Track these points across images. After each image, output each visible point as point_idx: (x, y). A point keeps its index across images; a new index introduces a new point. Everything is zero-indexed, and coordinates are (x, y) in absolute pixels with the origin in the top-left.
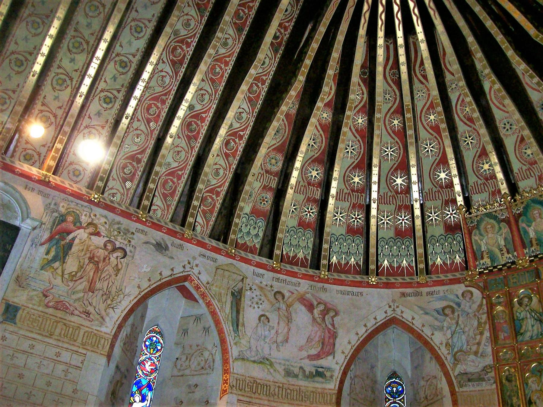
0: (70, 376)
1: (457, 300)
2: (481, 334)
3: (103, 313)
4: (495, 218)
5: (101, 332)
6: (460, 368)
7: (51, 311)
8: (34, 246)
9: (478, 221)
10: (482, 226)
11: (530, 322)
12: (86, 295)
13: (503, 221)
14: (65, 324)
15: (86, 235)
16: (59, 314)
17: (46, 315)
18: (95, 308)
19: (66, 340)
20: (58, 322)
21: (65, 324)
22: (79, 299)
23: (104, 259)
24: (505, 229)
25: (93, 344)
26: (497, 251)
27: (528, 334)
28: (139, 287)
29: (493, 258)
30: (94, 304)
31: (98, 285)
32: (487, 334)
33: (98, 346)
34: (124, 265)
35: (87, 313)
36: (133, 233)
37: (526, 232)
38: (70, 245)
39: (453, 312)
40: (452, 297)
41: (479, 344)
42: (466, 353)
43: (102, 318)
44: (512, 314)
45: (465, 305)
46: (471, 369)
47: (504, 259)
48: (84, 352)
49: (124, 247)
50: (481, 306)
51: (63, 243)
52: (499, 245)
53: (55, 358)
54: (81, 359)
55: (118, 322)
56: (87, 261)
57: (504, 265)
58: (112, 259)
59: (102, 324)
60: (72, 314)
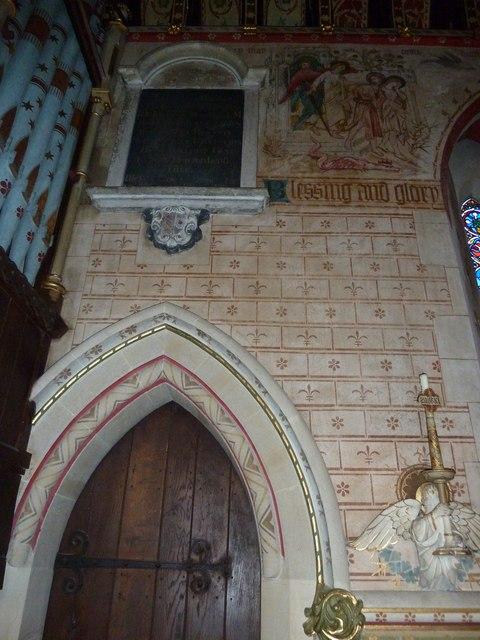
0: (402, 250)
3: (409, 156)
5: (420, 180)
7: (331, 174)
8: (271, 107)
12: (373, 142)
14: (361, 184)
15: (337, 76)
16: (347, 174)
17: (328, 181)
18: (394, 153)
19: (371, 203)
20: (349, 185)
21: (361, 184)
22: (365, 150)
23: (377, 95)
25: (416, 198)
28: (444, 113)
30: (391, 149)
31: (384, 126)
33: (424, 200)
34: (409, 93)
35: (387, 162)
36: (399, 57)
38: (321, 91)
43: (411, 162)
48: (409, 212)
49: (396, 74)
51: (308, 93)
53: (368, 230)
54: (407, 222)
55: (439, 162)
56: (353, 104)
58: (388, 92)
59: (416, 172)
60: (365, 169)
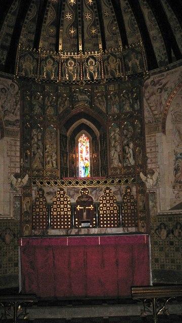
1: (8, 87)
2: (16, 105)
4: (33, 56)
6: (6, 118)
9: (25, 54)
10: (26, 57)
11: (37, 107)
13: (36, 59)
24: (35, 63)
26: (29, 71)
27: (36, 111)
29: (26, 74)
32: (19, 106)
37: (43, 69)
39: (6, 91)
40: (6, 84)
41: (15, 109)
42: (10, 112)
44: (31, 101)
45: (11, 90)
46: (10, 120)
47: (31, 75)
50: (17, 93)
52: (30, 69)
57: (31, 78)
